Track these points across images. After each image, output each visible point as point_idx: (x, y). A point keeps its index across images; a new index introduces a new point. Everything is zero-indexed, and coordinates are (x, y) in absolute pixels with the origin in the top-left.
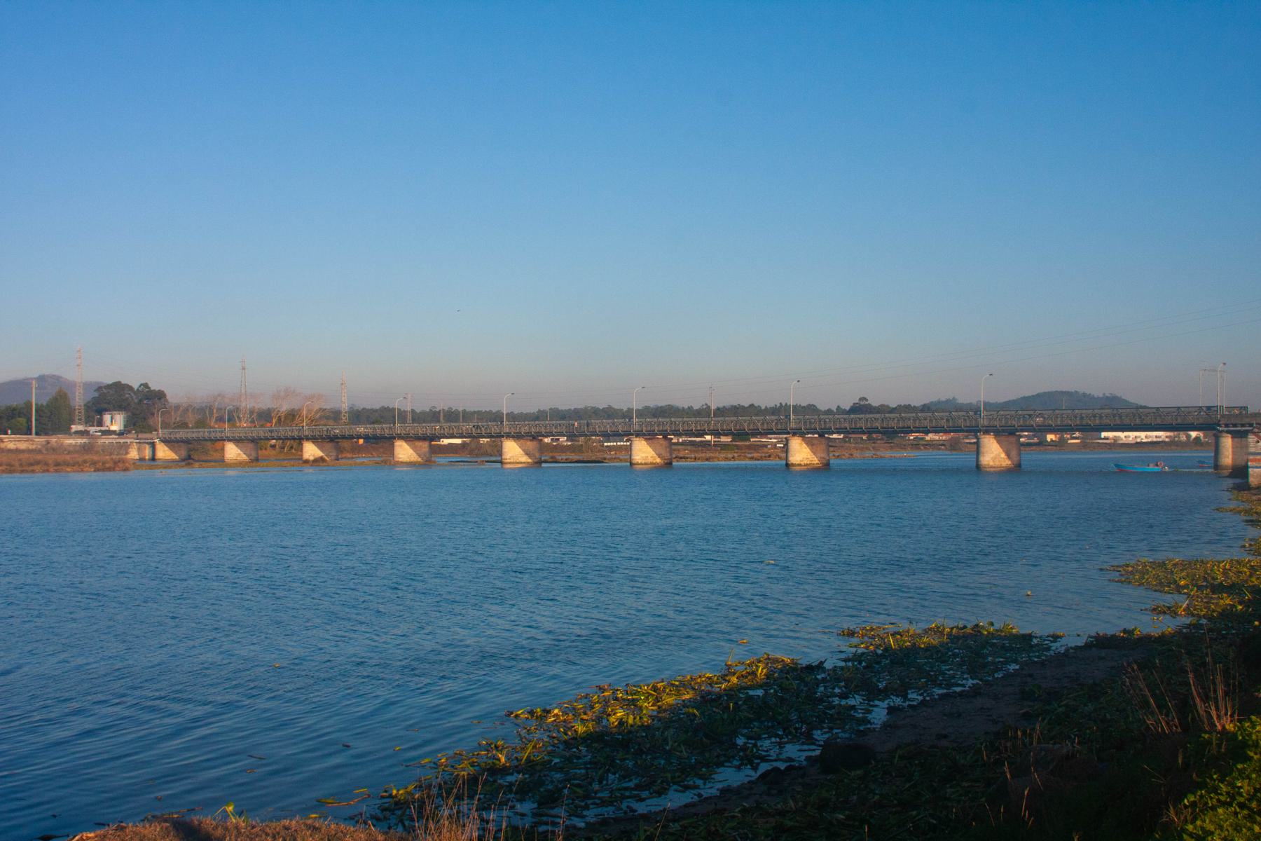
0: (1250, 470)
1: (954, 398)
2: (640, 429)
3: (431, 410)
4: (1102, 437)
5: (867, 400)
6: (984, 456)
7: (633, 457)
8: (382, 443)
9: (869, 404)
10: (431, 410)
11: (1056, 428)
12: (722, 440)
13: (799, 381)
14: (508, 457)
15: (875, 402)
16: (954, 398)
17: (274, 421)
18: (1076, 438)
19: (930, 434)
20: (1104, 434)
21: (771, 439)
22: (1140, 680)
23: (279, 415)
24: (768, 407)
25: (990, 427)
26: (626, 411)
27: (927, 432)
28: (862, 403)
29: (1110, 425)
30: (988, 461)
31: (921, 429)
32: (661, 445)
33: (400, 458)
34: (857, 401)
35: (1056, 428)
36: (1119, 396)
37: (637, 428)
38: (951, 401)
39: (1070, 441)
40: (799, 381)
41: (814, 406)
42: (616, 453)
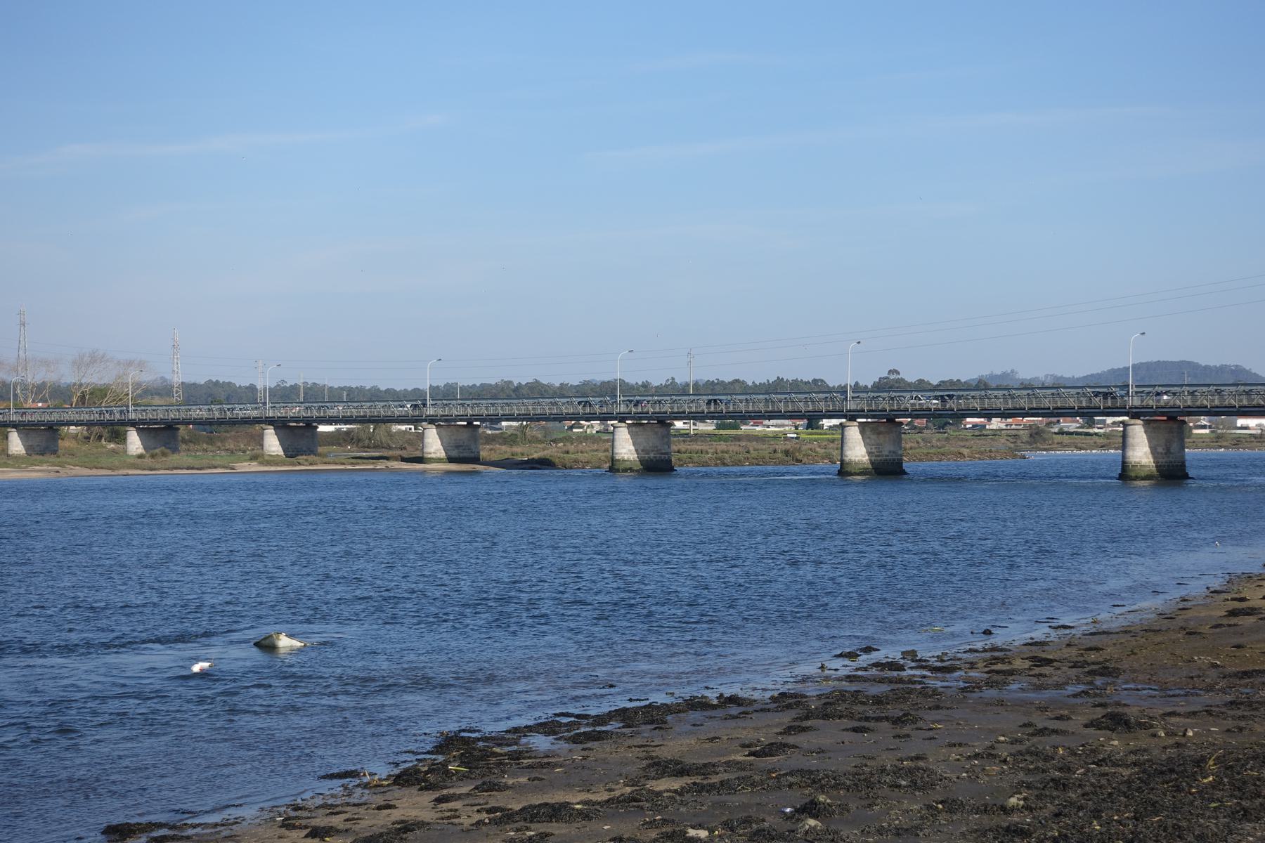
0: (904, 465)
1: (1012, 371)
2: (627, 411)
3: (278, 385)
4: (1239, 425)
5: (898, 373)
6: (1134, 450)
7: (616, 451)
8: (118, 435)
9: (903, 380)
10: (278, 385)
11: (1056, 411)
12: (700, 428)
13: (859, 343)
14: (432, 450)
15: (910, 377)
16: (1012, 371)
17: (75, 399)
18: (1204, 427)
19: (994, 420)
20: (1241, 422)
21: (768, 427)
22: (623, 727)
23: (82, 389)
24: (678, 381)
25: (1143, 408)
26: (558, 388)
27: (989, 417)
28: (892, 377)
29: (1206, 407)
30: (1141, 458)
31: (716, 415)
32: (656, 433)
33: (274, 452)
34: (886, 375)
35: (1056, 411)
36: (1248, 368)
37: (622, 410)
38: (1008, 374)
39: (1196, 431)
40: (859, 343)
41: (822, 381)
42: (564, 445)
